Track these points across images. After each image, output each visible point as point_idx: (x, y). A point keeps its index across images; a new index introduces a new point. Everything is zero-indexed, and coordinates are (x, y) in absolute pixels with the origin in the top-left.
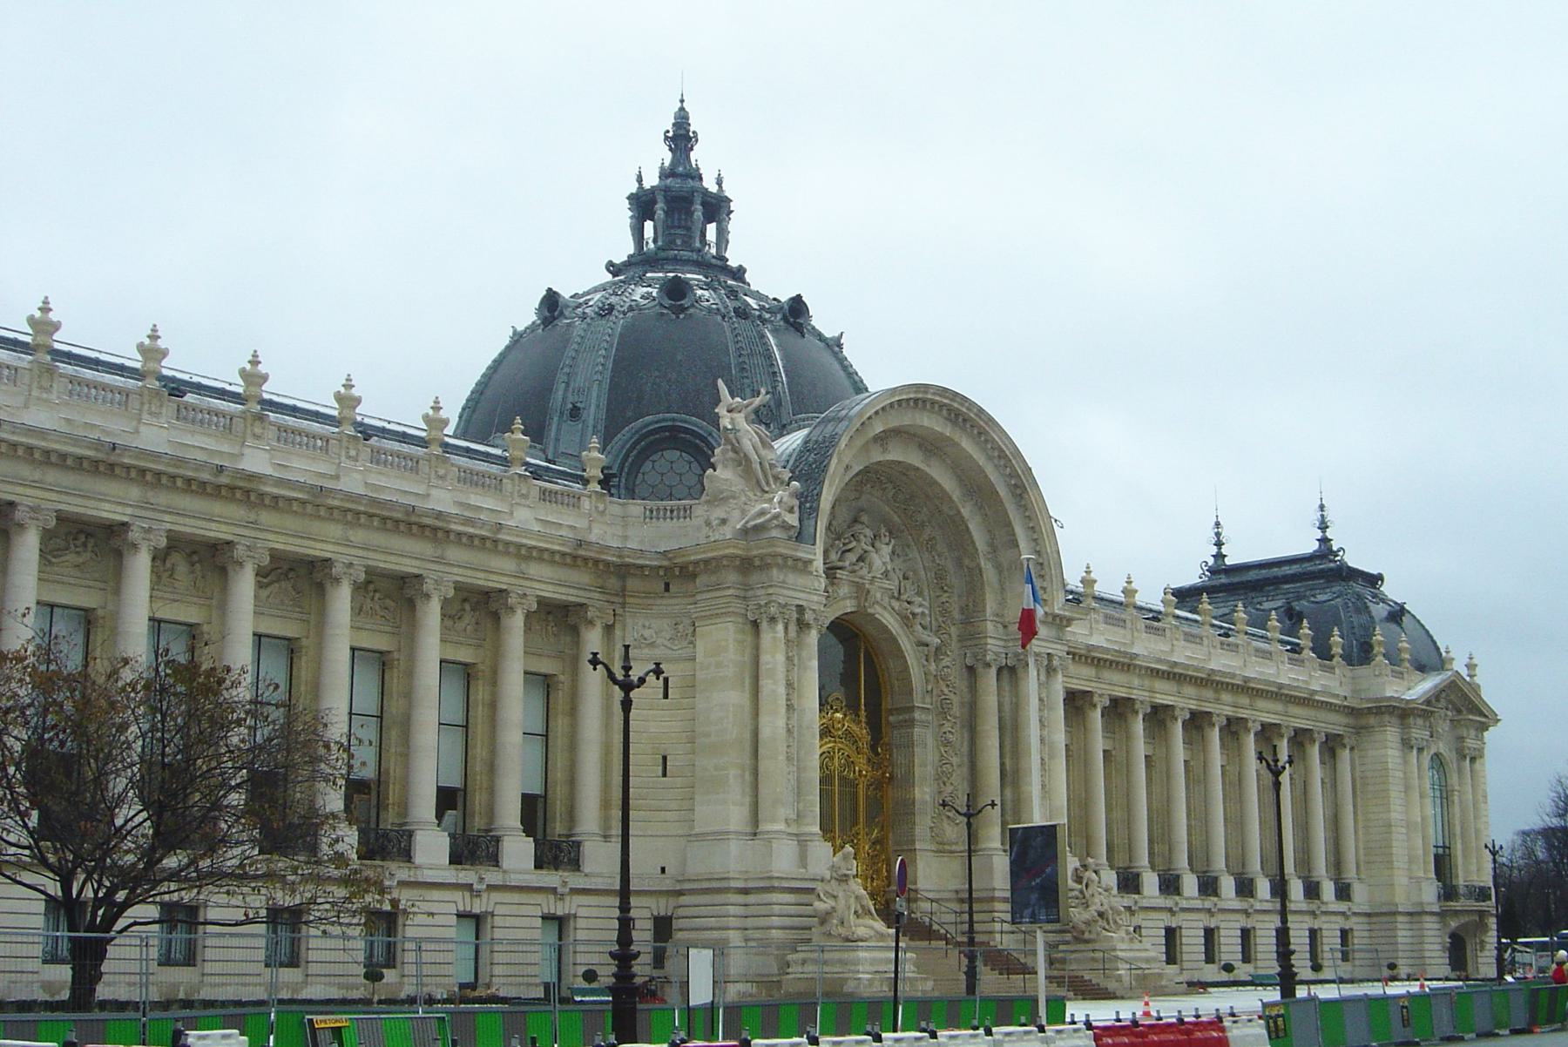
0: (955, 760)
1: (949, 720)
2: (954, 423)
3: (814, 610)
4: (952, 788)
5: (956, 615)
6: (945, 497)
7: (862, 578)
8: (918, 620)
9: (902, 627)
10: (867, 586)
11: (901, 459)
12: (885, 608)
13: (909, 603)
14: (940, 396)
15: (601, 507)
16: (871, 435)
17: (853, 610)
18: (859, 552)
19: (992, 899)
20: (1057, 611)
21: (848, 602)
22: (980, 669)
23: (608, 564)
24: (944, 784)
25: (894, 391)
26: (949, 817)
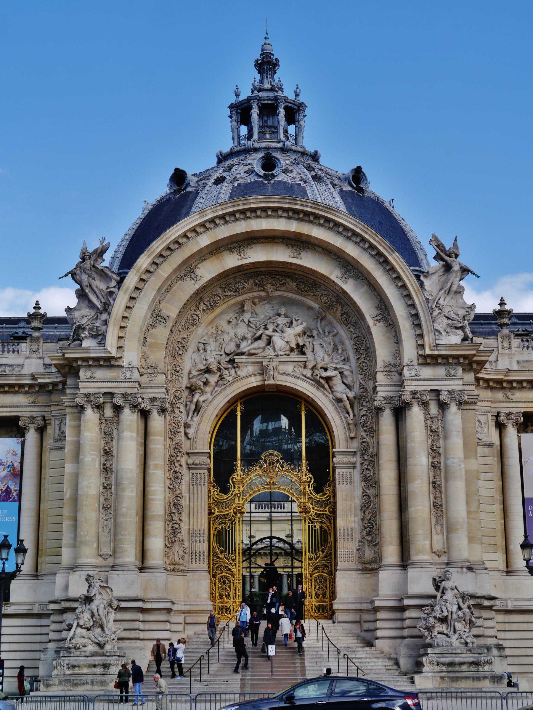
1: (366, 460)
3: (123, 394)
4: (370, 515)
7: (264, 357)
10: (264, 364)
12: (297, 377)
13: (326, 370)
14: (264, 202)
15: (34, 348)
16: (195, 249)
17: (259, 383)
18: (264, 337)
19: (376, 610)
20: (428, 352)
21: (253, 379)
23: (31, 386)
26: (368, 541)
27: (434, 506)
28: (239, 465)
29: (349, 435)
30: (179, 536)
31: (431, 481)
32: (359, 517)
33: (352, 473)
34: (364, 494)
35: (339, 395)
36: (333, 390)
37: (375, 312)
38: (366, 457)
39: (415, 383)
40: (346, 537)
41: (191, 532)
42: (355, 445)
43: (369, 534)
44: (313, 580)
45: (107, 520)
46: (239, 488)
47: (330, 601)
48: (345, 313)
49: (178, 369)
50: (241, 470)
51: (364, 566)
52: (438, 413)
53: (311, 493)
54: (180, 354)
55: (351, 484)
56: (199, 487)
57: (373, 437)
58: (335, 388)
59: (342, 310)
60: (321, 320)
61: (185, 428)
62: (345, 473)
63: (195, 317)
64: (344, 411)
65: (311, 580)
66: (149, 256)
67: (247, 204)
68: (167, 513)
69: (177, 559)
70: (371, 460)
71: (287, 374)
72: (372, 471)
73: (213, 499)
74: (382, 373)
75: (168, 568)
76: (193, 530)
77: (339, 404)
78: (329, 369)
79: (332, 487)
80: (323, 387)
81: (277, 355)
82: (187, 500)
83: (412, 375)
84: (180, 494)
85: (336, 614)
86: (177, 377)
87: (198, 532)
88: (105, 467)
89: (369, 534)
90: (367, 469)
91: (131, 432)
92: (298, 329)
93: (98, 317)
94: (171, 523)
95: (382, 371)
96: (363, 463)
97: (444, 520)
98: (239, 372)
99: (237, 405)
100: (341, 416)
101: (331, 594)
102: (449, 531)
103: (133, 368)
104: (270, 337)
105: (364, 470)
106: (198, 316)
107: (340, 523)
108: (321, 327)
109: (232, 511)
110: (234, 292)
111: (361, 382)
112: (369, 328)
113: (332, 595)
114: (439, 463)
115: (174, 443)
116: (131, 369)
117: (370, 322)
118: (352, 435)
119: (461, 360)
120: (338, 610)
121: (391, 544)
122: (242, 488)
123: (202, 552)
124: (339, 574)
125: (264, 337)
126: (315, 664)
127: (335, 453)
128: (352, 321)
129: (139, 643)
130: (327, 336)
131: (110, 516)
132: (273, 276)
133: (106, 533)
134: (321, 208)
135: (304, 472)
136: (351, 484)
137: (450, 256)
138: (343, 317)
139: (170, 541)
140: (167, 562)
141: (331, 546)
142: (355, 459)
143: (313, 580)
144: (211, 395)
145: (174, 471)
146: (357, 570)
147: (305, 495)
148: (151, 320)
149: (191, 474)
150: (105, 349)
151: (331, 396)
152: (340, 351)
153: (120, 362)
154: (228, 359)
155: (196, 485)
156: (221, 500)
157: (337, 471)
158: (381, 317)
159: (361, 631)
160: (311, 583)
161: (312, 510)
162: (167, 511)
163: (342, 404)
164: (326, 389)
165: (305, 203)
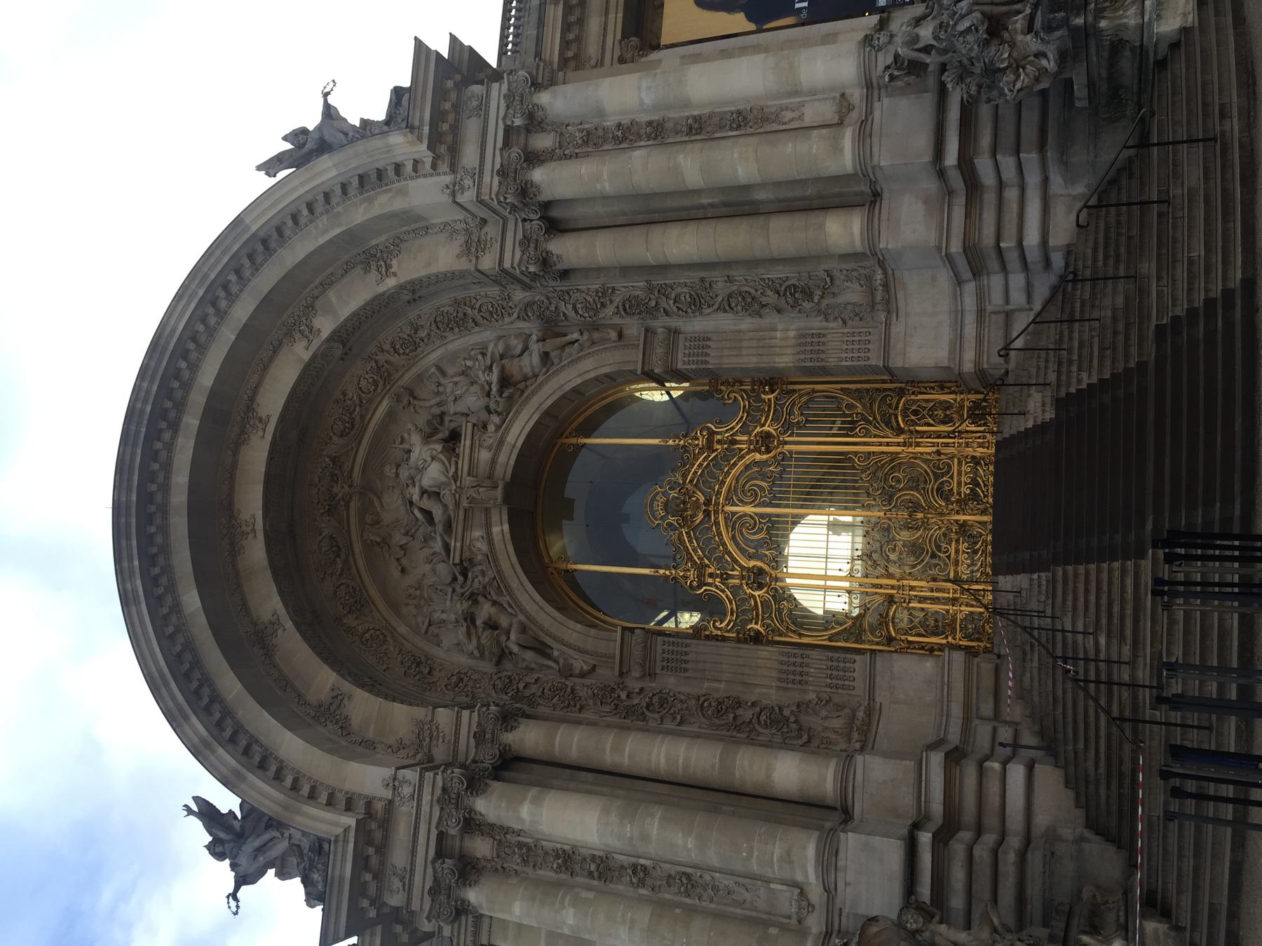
0: (721, 289)
2: (180, 406)
4: (769, 293)
5: (494, 291)
6: (310, 372)
7: (457, 504)
8: (514, 368)
9: (528, 399)
11: (259, 488)
12: (501, 442)
16: (202, 620)
17: (505, 517)
18: (426, 503)
20: (424, 146)
21: (496, 530)
22: (560, 267)
24: (764, 306)
25: (126, 600)
26: (822, 297)
27: (739, 127)
28: (667, 573)
29: (615, 342)
30: (786, 713)
31: (687, 138)
32: (777, 320)
33: (688, 336)
34: (727, 308)
35: (536, 359)
36: (531, 374)
37: (373, 276)
38: (653, 303)
39: (487, 179)
40: (817, 348)
41: (784, 685)
42: (633, 328)
43: (808, 295)
44: (912, 428)
45: (716, 889)
46: (711, 575)
47: (962, 393)
48: (393, 346)
49: (454, 679)
50: (675, 568)
51: (879, 307)
52: (553, 134)
53: (732, 428)
54: (430, 673)
55: (709, 339)
56: (690, 657)
57: (614, 288)
58: (527, 370)
59: (388, 352)
60: (415, 398)
61: (571, 676)
62: (687, 351)
63: (367, 635)
64: (567, 350)
65: (911, 432)
66: (186, 718)
67: (128, 508)
68: (734, 733)
69: (837, 723)
70: (659, 291)
71: (493, 462)
72: (679, 290)
73: (728, 631)
74: (480, 260)
75: (858, 745)
76: (780, 680)
77: (556, 361)
78: (488, 379)
79: (723, 388)
80: (522, 392)
81: (455, 478)
82: (716, 685)
83: (471, 186)
84: (698, 700)
85: (985, 366)
86: (471, 683)
87: (785, 667)
88: (596, 874)
89: (808, 295)
90: (675, 302)
91: (523, 800)
92: (415, 439)
93: (296, 843)
94: (757, 727)
95: (477, 258)
96: (664, 309)
97: (770, 103)
98: (479, 557)
99: (555, 569)
100: (579, 358)
101: (946, 391)
102: (796, 93)
103: (395, 779)
104: (423, 492)
105: (679, 309)
106: (369, 630)
107: (784, 360)
108: (429, 400)
109: (756, 593)
110: (338, 556)
111: (515, 315)
112: (401, 287)
113: (947, 388)
114: (650, 123)
115: (591, 702)
116: (396, 783)
117: (391, 282)
118: (613, 335)
119: (450, 84)
120: (977, 363)
121: (821, 227)
122: (711, 570)
123: (830, 663)
124: (897, 362)
125: (426, 503)
126: (1109, 352)
127: (646, 369)
128: (408, 332)
129: (1036, 860)
130: (445, 389)
131: (707, 877)
132: (317, 479)
133: (747, 896)
134: (153, 364)
135: (690, 441)
136: (709, 339)
137: (304, 145)
138: (401, 351)
139: (793, 734)
140: (843, 746)
141: (842, 389)
142: (660, 330)
143: (912, 428)
144: (516, 616)
145: (648, 708)
146: (888, 325)
147: (734, 442)
148: (330, 726)
149: (664, 672)
150: (336, 841)
151: (541, 378)
152: (469, 363)
153: (379, 806)
154: (460, 578)
155: (686, 662)
156: (732, 614)
157: (680, 366)
158: (382, 263)
159: (1031, 309)
160: (918, 432)
161: (766, 428)
162: (729, 733)
163: (552, 354)
164: (526, 387)
165: (142, 394)
